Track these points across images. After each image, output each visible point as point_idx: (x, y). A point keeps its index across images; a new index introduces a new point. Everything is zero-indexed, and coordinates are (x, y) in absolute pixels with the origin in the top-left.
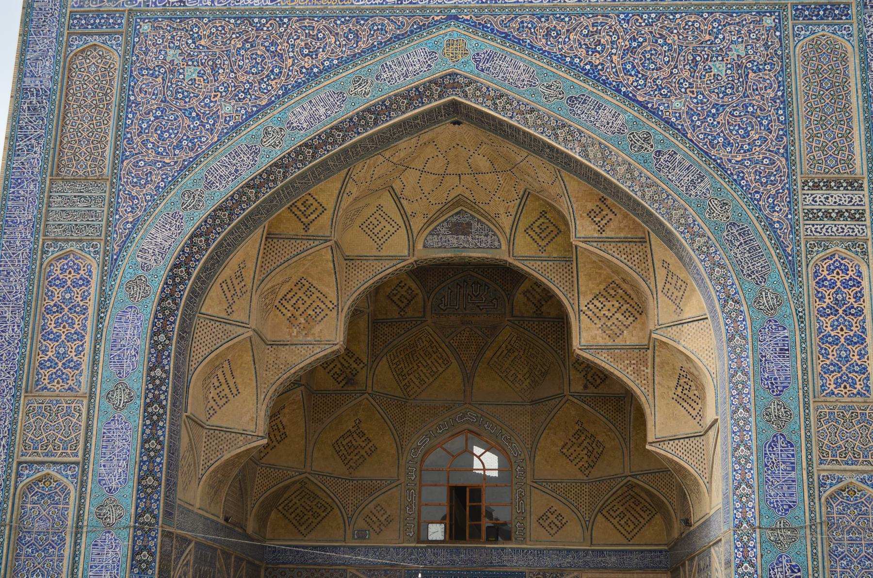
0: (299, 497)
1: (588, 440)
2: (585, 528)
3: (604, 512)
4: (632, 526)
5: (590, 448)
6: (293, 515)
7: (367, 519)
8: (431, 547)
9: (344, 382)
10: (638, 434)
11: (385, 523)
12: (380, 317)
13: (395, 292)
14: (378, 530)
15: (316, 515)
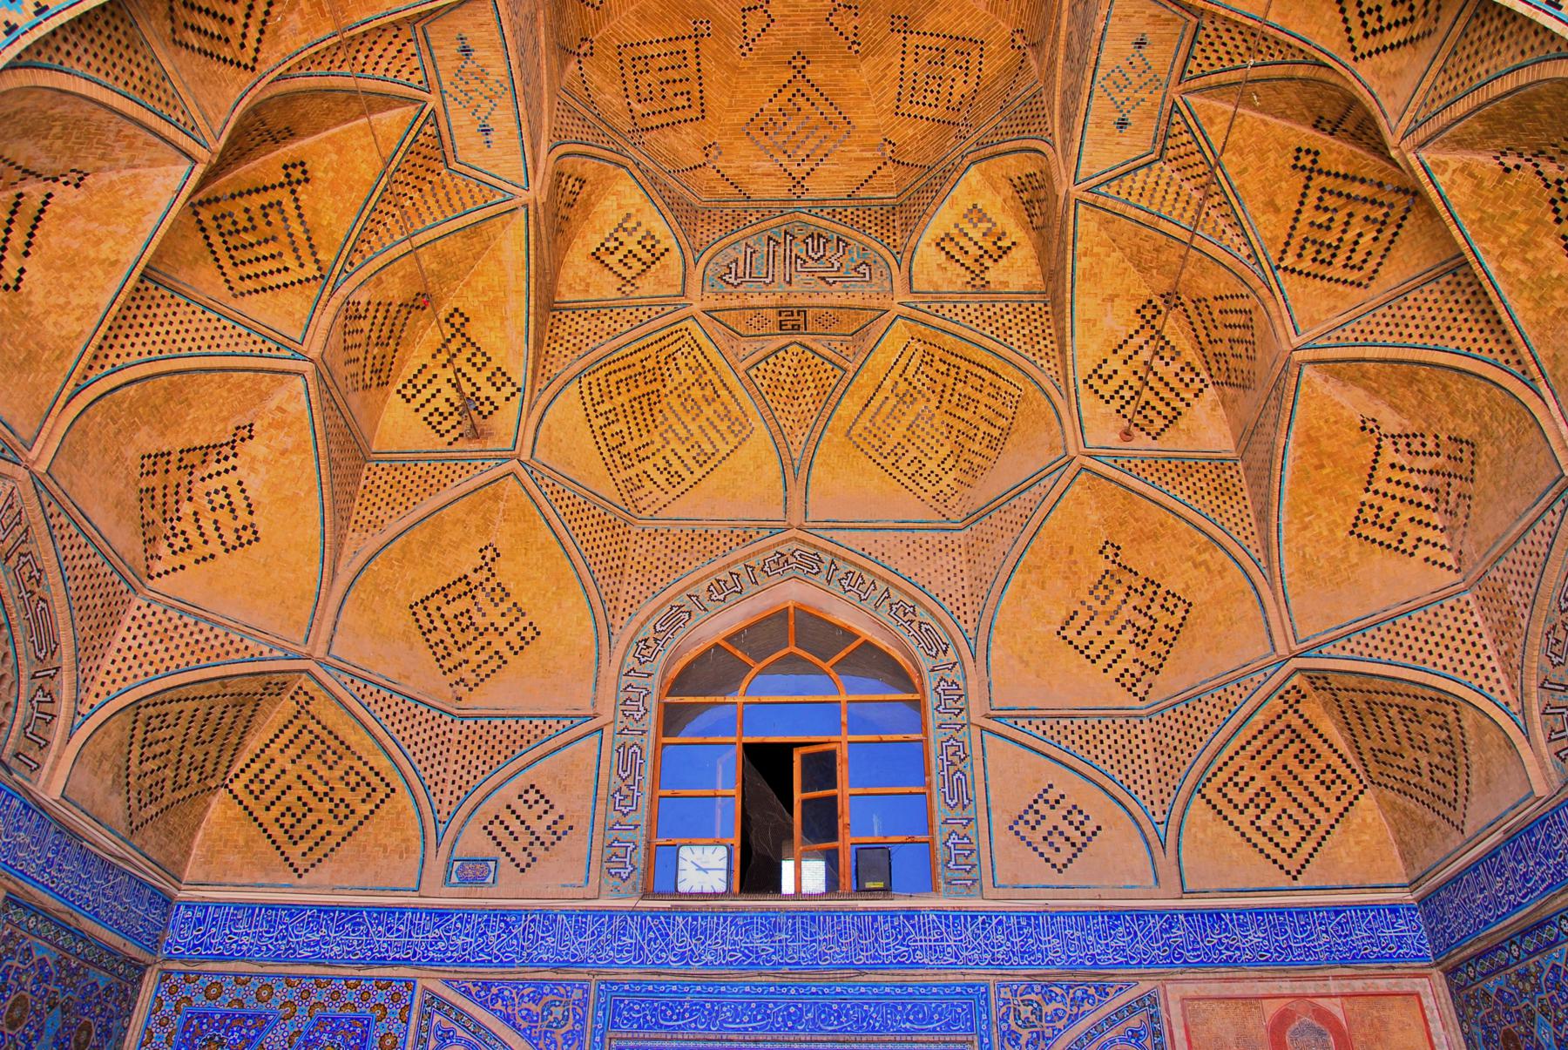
0: (293, 751)
1: (1135, 600)
2: (1156, 845)
3: (1210, 792)
4: (1296, 835)
5: (1144, 623)
6: (275, 811)
7: (497, 829)
8: (683, 911)
9: (455, 433)
10: (1305, 528)
11: (548, 838)
12: (569, 297)
13: (611, 244)
14: (523, 859)
15: (342, 811)
